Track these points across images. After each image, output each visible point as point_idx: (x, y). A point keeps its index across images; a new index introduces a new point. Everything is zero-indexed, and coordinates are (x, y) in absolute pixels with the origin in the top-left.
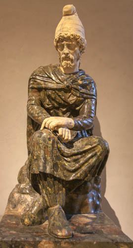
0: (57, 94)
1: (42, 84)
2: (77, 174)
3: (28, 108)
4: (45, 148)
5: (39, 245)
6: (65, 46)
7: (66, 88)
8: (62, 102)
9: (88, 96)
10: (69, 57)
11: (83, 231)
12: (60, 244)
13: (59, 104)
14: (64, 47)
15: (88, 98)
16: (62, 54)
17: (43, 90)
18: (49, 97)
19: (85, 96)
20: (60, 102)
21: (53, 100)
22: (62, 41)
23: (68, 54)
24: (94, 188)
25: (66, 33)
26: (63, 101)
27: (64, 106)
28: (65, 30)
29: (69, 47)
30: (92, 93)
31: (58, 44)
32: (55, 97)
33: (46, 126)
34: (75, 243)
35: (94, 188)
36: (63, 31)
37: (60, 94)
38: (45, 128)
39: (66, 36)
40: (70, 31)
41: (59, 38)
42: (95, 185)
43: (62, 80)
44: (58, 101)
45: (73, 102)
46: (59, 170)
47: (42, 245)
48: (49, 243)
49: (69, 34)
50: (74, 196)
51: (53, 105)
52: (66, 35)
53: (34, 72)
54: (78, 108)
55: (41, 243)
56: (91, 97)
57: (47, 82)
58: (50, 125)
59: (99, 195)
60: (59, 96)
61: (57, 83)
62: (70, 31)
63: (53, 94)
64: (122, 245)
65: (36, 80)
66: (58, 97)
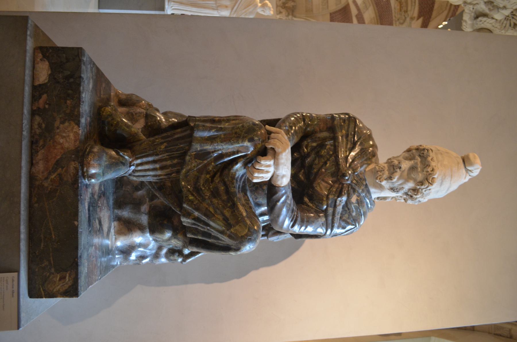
0: (328, 160)
1: (341, 131)
2: (193, 195)
3: (299, 113)
4: (236, 133)
5: (72, 123)
6: (412, 162)
7: (340, 174)
8: (315, 170)
9: (330, 218)
10: (394, 172)
11: (91, 208)
12: (74, 161)
13: (311, 166)
14: (411, 160)
15: (326, 216)
16: (398, 160)
17: (332, 135)
18: (322, 146)
19: (330, 210)
20: (314, 166)
21: (318, 155)
22: (420, 156)
23: (400, 168)
24: (160, 248)
25: (435, 159)
26: (319, 170)
27: (307, 175)
28: (440, 156)
29: (413, 169)
30: (336, 225)
31: (414, 151)
32: (322, 156)
33: (272, 135)
34: (76, 186)
35: (160, 248)
36: (436, 154)
37: (328, 165)
38: (269, 133)
39: (429, 159)
40: (439, 165)
41: (424, 149)
42: (164, 251)
43: (353, 166)
44: (317, 162)
45: (318, 189)
46: (199, 161)
47: (73, 128)
48: (75, 141)
49: (433, 164)
50: (145, 208)
51: (308, 155)
52: (432, 159)
53: (359, 120)
54: (306, 199)
55: (76, 127)
56: (330, 221)
57: (347, 140)
58: (276, 140)
59: (148, 260)
60: (326, 163)
61: (346, 158)
62: (439, 165)
63: (328, 153)
64: (73, 276)
65: (347, 122)
66: (323, 161)
